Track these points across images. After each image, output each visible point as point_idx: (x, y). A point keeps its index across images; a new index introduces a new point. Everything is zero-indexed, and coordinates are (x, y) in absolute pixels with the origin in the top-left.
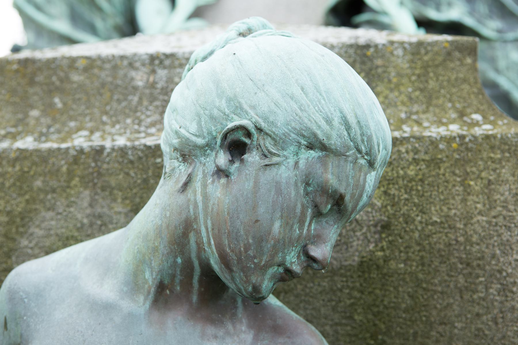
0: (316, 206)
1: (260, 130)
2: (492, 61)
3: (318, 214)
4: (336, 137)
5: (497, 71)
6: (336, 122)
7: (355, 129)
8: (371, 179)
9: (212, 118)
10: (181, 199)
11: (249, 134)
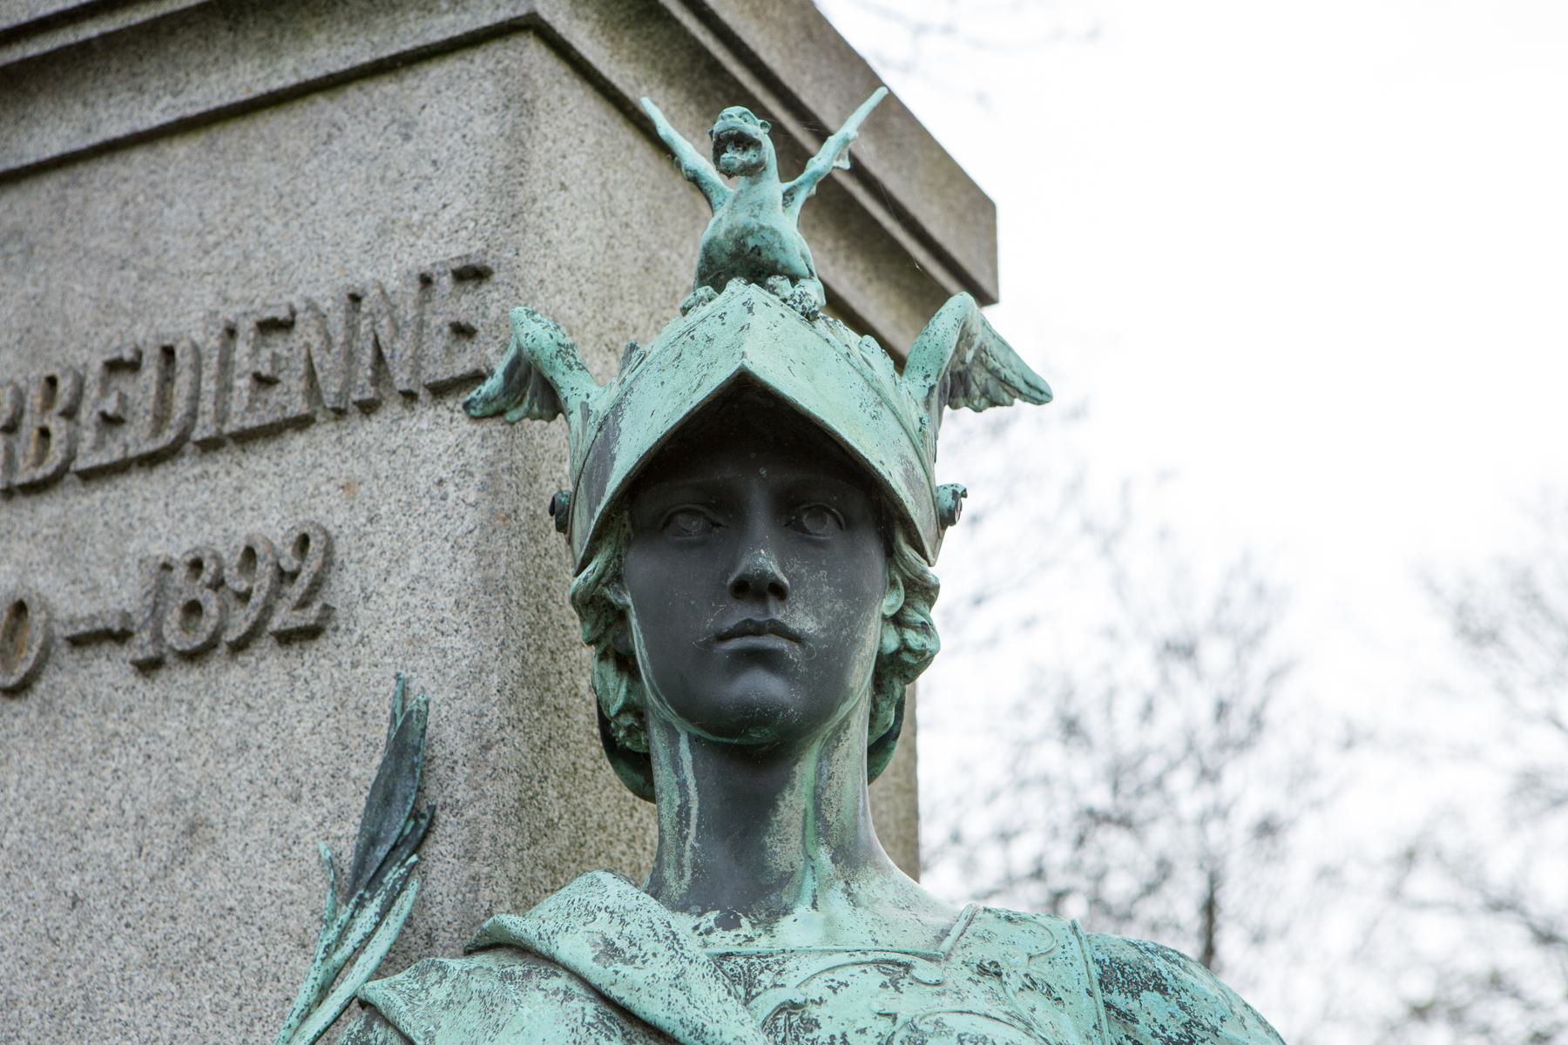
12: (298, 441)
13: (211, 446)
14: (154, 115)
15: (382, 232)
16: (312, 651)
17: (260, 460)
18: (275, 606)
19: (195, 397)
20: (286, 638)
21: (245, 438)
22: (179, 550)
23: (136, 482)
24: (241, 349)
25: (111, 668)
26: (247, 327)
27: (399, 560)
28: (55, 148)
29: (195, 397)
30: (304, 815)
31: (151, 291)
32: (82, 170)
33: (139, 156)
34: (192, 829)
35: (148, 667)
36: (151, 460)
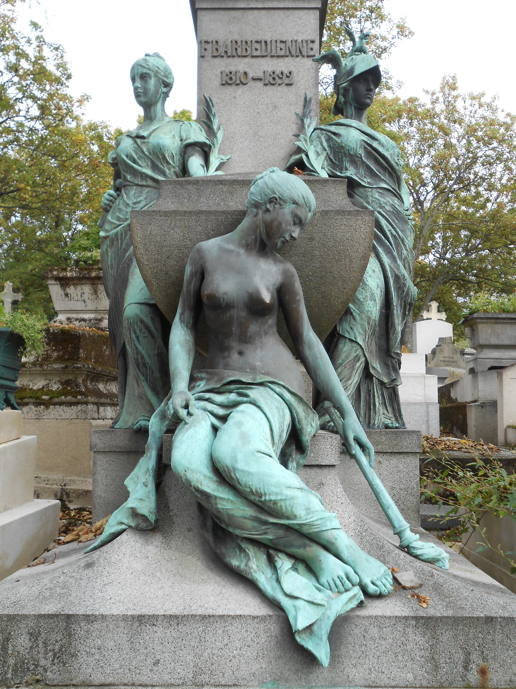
0: (294, 221)
1: (279, 198)
2: (366, 198)
3: (295, 224)
4: (301, 201)
5: (368, 203)
6: (301, 196)
7: (306, 199)
8: (310, 215)
9: (266, 195)
10: (255, 219)
11: (276, 199)
12: (287, 59)
13: (272, 56)
14: (260, 6)
15: (298, 32)
16: (291, 87)
17: (281, 60)
18: (283, 80)
19: (271, 49)
20: (287, 85)
21: (278, 57)
22: (270, 70)
23: (260, 59)
24: (278, 44)
25: (260, 84)
26: (278, 41)
27: (303, 78)
28: (242, 6)
29: (271, 49)
30: (292, 107)
31: (260, 32)
32: (247, 11)
33: (256, 11)
34: (275, 106)
35: (266, 85)
36: (263, 56)
